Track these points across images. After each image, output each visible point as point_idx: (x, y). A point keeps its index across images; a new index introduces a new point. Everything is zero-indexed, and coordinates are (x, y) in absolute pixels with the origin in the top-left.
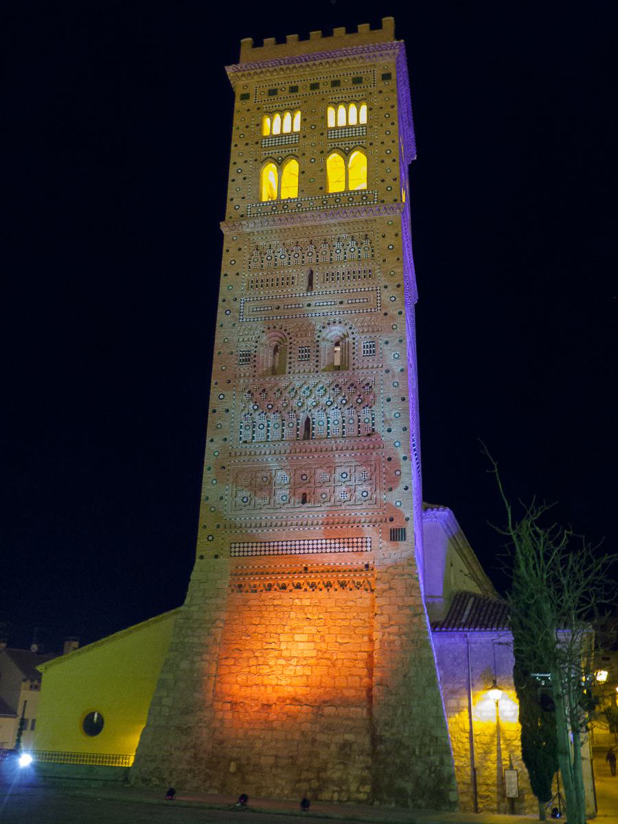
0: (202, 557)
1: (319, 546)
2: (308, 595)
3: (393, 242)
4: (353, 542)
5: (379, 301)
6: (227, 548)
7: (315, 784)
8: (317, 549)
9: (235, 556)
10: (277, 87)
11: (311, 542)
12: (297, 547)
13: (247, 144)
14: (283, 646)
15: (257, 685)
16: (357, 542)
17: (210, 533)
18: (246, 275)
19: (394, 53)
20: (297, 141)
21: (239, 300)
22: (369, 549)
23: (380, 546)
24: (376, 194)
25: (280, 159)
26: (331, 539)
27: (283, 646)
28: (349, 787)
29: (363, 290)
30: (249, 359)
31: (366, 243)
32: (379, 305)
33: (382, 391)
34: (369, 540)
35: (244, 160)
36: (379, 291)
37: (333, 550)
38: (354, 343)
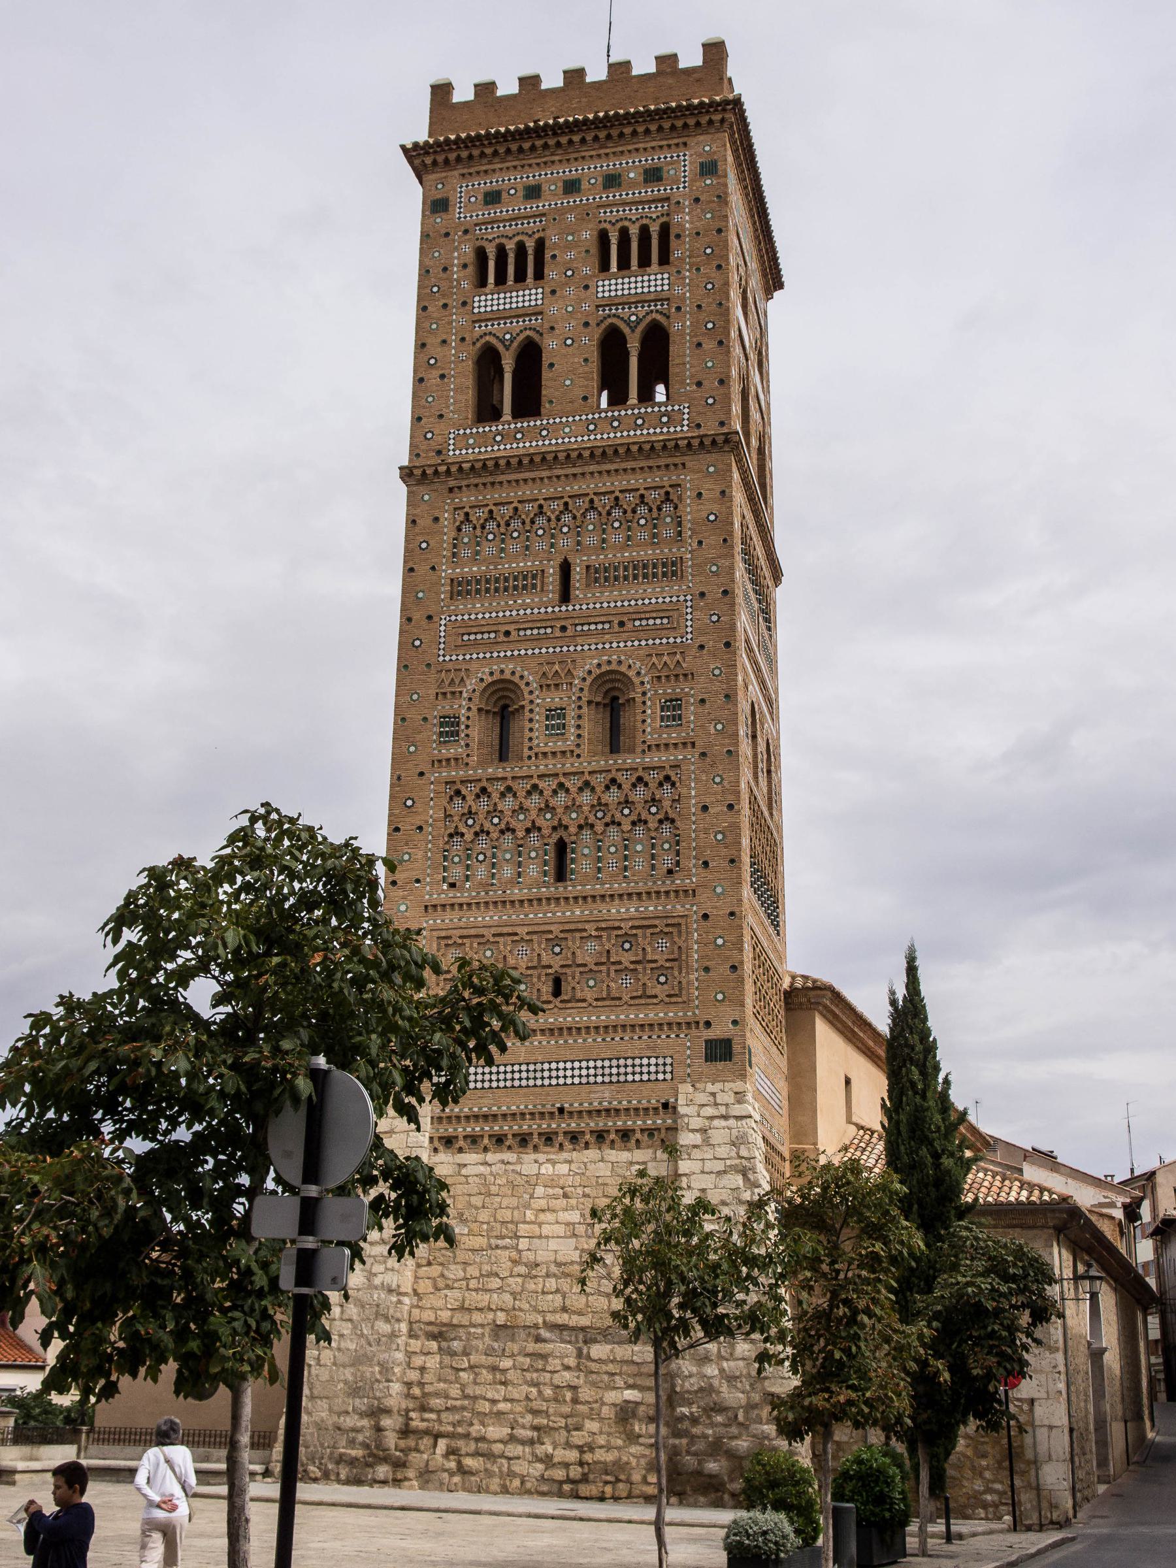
2: (565, 1155)
3: (715, 508)
4: (641, 1065)
5: (689, 623)
7: (575, 1472)
8: (580, 1076)
11: (569, 1065)
12: (546, 1074)
13: (445, 306)
14: (523, 1244)
15: (480, 1310)
16: (649, 1065)
18: (447, 571)
19: (722, 121)
20: (540, 302)
21: (435, 619)
22: (668, 1076)
23: (689, 1071)
24: (686, 410)
25: (508, 337)
26: (603, 1060)
27: (523, 1244)
28: (630, 1475)
29: (660, 600)
30: (458, 731)
31: (667, 508)
32: (689, 630)
33: (693, 793)
35: (439, 340)
36: (689, 604)
37: (607, 1079)
38: (644, 703)
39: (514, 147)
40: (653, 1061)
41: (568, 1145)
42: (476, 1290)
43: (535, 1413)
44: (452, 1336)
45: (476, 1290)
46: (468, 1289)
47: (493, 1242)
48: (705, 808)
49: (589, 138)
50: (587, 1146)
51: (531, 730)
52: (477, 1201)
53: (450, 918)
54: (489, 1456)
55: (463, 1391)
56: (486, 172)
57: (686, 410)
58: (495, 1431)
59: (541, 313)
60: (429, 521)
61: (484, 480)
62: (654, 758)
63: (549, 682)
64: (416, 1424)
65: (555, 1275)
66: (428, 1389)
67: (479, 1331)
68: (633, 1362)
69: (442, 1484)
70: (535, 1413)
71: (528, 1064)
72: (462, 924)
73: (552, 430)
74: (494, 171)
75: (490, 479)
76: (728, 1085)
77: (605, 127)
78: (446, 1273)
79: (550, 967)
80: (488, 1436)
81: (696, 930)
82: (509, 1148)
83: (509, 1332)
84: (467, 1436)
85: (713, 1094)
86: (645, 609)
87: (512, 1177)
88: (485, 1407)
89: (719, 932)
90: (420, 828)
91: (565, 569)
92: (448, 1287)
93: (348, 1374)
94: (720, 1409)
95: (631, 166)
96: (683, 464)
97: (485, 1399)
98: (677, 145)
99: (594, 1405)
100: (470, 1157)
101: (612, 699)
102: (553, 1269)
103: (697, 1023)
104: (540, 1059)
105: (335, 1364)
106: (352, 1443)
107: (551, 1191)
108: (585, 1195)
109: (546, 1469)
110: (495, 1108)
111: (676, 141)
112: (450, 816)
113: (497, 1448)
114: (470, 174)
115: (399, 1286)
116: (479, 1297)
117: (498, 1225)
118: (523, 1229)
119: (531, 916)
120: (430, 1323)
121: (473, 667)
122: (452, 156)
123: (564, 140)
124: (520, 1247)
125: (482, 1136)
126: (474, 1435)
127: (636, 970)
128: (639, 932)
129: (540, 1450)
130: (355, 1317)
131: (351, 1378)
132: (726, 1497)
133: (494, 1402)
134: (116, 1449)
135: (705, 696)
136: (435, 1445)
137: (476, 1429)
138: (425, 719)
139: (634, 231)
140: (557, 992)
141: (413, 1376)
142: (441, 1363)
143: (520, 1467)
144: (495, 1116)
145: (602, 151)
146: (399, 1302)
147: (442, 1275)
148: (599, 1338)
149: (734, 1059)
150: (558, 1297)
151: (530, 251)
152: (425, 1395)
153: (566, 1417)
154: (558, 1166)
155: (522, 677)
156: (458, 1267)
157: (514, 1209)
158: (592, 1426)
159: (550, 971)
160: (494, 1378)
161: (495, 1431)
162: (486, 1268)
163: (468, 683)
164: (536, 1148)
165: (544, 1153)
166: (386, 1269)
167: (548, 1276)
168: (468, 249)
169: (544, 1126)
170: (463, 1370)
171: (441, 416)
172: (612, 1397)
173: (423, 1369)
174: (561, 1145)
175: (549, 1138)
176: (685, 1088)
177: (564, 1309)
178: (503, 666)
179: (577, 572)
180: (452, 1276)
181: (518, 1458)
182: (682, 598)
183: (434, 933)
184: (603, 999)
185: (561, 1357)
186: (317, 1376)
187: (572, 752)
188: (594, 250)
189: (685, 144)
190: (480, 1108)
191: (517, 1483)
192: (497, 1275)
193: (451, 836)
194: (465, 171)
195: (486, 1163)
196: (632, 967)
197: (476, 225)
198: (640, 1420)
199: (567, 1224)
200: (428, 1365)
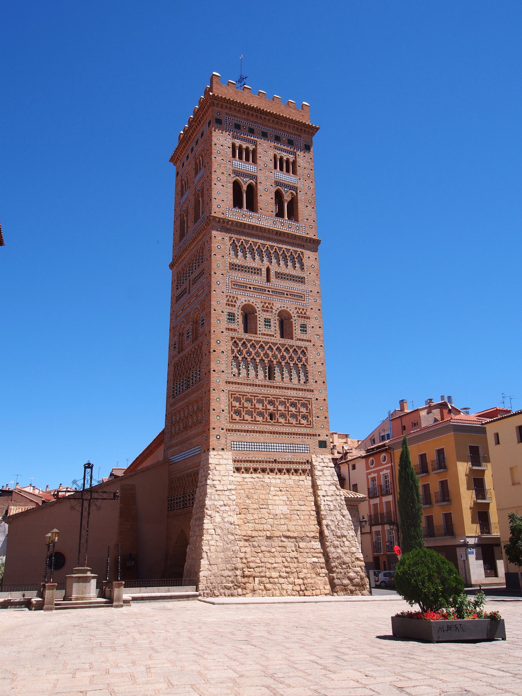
0: (214, 449)
1: (282, 448)
2: (278, 476)
6: (229, 445)
7: (303, 587)
10: (242, 124)
17: (217, 433)
27: (270, 507)
34: (308, 446)
40: (303, 446)
43: (286, 567)
47: (261, 506)
54: (275, 583)
58: (275, 574)
60: (220, 238)
62: (300, 343)
66: (249, 560)
67: (262, 538)
69: (260, 594)
70: (286, 567)
72: (239, 390)
76: (326, 456)
80: (273, 576)
82: (259, 473)
87: (262, 483)
88: (269, 566)
91: (268, 270)
92: (248, 522)
100: (245, 475)
102: (282, 516)
103: (316, 435)
106: (227, 581)
113: (276, 580)
117: (261, 500)
120: (245, 536)
121: (239, 297)
126: (267, 576)
129: (291, 580)
131: (223, 557)
137: (268, 574)
141: (242, 555)
143: (284, 586)
150: (285, 526)
152: (248, 562)
158: (305, 571)
159: (270, 411)
161: (275, 574)
162: (260, 516)
163: (237, 302)
164: (268, 474)
172: (308, 560)
175: (272, 471)
176: (314, 456)
179: (272, 273)
183: (230, 392)
187: (273, 336)
188: (273, 161)
189: (300, 136)
191: (285, 591)
194: (228, 112)
199: (284, 501)
200: (247, 551)
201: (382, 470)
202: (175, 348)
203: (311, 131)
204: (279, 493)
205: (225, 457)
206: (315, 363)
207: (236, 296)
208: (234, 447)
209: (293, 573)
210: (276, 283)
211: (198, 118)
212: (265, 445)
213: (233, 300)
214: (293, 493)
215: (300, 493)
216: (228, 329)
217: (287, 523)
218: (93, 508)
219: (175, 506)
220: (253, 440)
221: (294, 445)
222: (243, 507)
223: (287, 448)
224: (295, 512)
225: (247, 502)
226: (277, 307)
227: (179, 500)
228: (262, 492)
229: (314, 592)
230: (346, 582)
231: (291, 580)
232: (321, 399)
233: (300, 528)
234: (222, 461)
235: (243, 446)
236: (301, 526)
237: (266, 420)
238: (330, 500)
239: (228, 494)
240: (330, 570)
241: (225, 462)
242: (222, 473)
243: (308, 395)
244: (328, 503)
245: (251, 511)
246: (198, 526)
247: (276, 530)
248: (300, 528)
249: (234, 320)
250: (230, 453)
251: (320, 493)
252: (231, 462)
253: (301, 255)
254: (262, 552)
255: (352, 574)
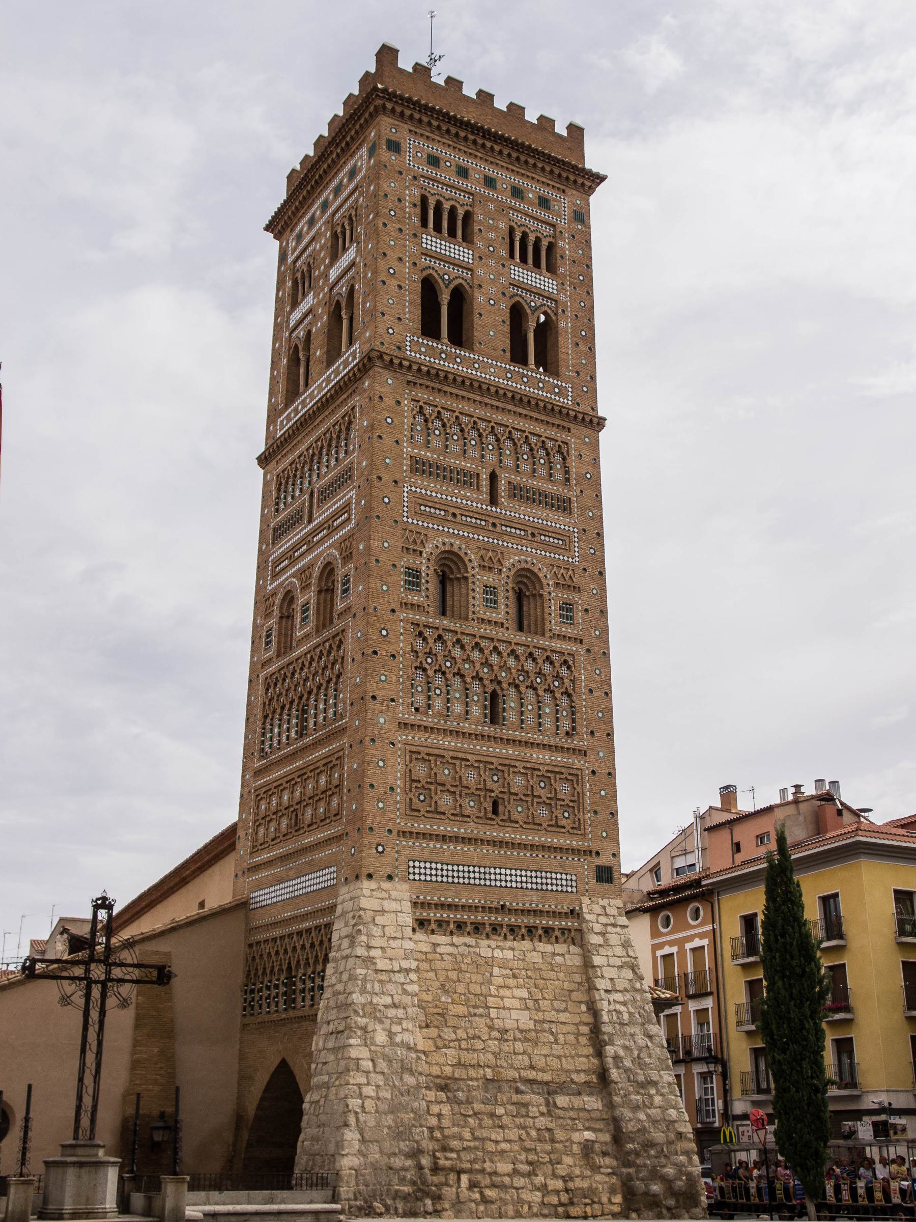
0: (370, 876)
1: (519, 879)
2: (509, 944)
6: (404, 867)
7: (564, 1198)
9: (414, 880)
17: (379, 840)
22: (574, 890)
27: (493, 1013)
28: (600, 1198)
34: (574, 878)
39: (453, 130)
41: (510, 937)
42: (467, 1050)
43: (527, 1150)
44: (456, 1087)
45: (467, 1050)
46: (461, 1049)
48: (591, 691)
49: (506, 152)
50: (523, 939)
51: (474, 598)
52: (453, 975)
53: (418, 737)
55: (473, 1134)
56: (428, 137)
57: (570, 390)
58: (504, 1167)
59: (471, 270)
60: (393, 403)
61: (432, 385)
62: (558, 645)
63: (485, 564)
64: (442, 1162)
65: (520, 1040)
66: (447, 1132)
67: (475, 1084)
68: (585, 1110)
69: (471, 1212)
70: (527, 1150)
71: (479, 867)
73: (484, 367)
74: (434, 140)
75: (437, 386)
77: (518, 150)
78: (442, 1034)
79: (493, 791)
80: (499, 1170)
81: (588, 782)
82: (469, 933)
83: (496, 1085)
84: (483, 1171)
85: (604, 907)
86: (548, 529)
88: (491, 1147)
89: (603, 786)
90: (393, 656)
92: (446, 1046)
93: (389, 1120)
94: (650, 1144)
95: (533, 189)
96: (569, 429)
97: (491, 1140)
98: (558, 189)
99: (567, 1144)
101: (526, 589)
102: (518, 1035)
103: (591, 852)
104: (488, 864)
105: (377, 1111)
106: (402, 1180)
107: (505, 972)
108: (528, 977)
109: (543, 1196)
110: (457, 900)
111: (558, 186)
112: (416, 652)
113: (507, 1180)
114: (416, 133)
115: (415, 1045)
116: (470, 1056)
117: (472, 997)
118: (491, 1001)
119: (478, 747)
120: (438, 1077)
121: (431, 534)
122: (408, 112)
123: (488, 144)
124: (492, 1016)
125: (448, 922)
126: (488, 1170)
127: (550, 804)
128: (552, 775)
129: (539, 1180)
130: (385, 1071)
131: (393, 1124)
132: (664, 1211)
133: (497, 1142)
134: (215, 1195)
135: (588, 607)
136: (459, 1179)
138: (394, 566)
139: (532, 238)
140: (495, 812)
141: (433, 1121)
142: (452, 1110)
143: (526, 1196)
144: (456, 906)
145: (510, 167)
146: (419, 1058)
147: (440, 1037)
148: (559, 1091)
149: (615, 882)
151: (460, 217)
152: (445, 1137)
153: (548, 1154)
154: (505, 951)
155: (466, 553)
156: (450, 1029)
157: (481, 984)
158: (568, 1160)
159: (493, 794)
160: (494, 1123)
162: (471, 1031)
163: (426, 545)
164: (488, 936)
165: (494, 940)
166: (403, 1029)
167: (515, 1040)
168: (416, 192)
169: (493, 918)
170: (469, 1116)
171: (400, 319)
172: (576, 1137)
173: (439, 1116)
174: (505, 935)
176: (585, 900)
177: (532, 1067)
178: (452, 541)
180: (447, 1038)
181: (523, 1188)
182: (571, 529)
183: (408, 747)
184: (529, 823)
185: (538, 1106)
186: (365, 1122)
187: (502, 624)
188: (507, 240)
189: (564, 191)
190: (446, 898)
191: (526, 1208)
192: (479, 1038)
193: (416, 668)
194: (413, 128)
195: (453, 945)
196: (548, 802)
197: (422, 176)
198: (597, 1155)
199: (521, 999)
200: (443, 1112)
201: (690, 939)
202: (267, 643)
203: (588, 184)
204: (511, 982)
205: (394, 894)
206: (591, 691)
207: (423, 532)
208: (414, 873)
209: (544, 1164)
210: (510, 509)
211: (344, 137)
212: (482, 870)
213: (418, 541)
214: (541, 983)
215: (556, 983)
216: (405, 605)
217: (530, 1050)
218: (111, 1002)
219: (265, 1005)
220: (456, 859)
221: (544, 874)
222: (435, 1011)
223: (529, 880)
224: (546, 1026)
225: (443, 999)
226: (511, 561)
227: (274, 992)
228: (475, 978)
229: (588, 1209)
230: (656, 1188)
231: (539, 1180)
232: (602, 771)
233: (555, 1063)
234: (389, 905)
235: (434, 872)
236: (559, 1057)
237: (486, 813)
238: (621, 999)
239: (402, 980)
240: (625, 1160)
241: (395, 906)
242: (390, 931)
243: (577, 762)
244: (618, 1007)
245: (452, 1022)
246: (335, 1050)
247: (505, 1064)
248: (555, 1063)
249: (418, 585)
250: (405, 886)
251: (602, 984)
252: (407, 907)
253: (564, 450)
254: (475, 1114)
255: (670, 1171)
